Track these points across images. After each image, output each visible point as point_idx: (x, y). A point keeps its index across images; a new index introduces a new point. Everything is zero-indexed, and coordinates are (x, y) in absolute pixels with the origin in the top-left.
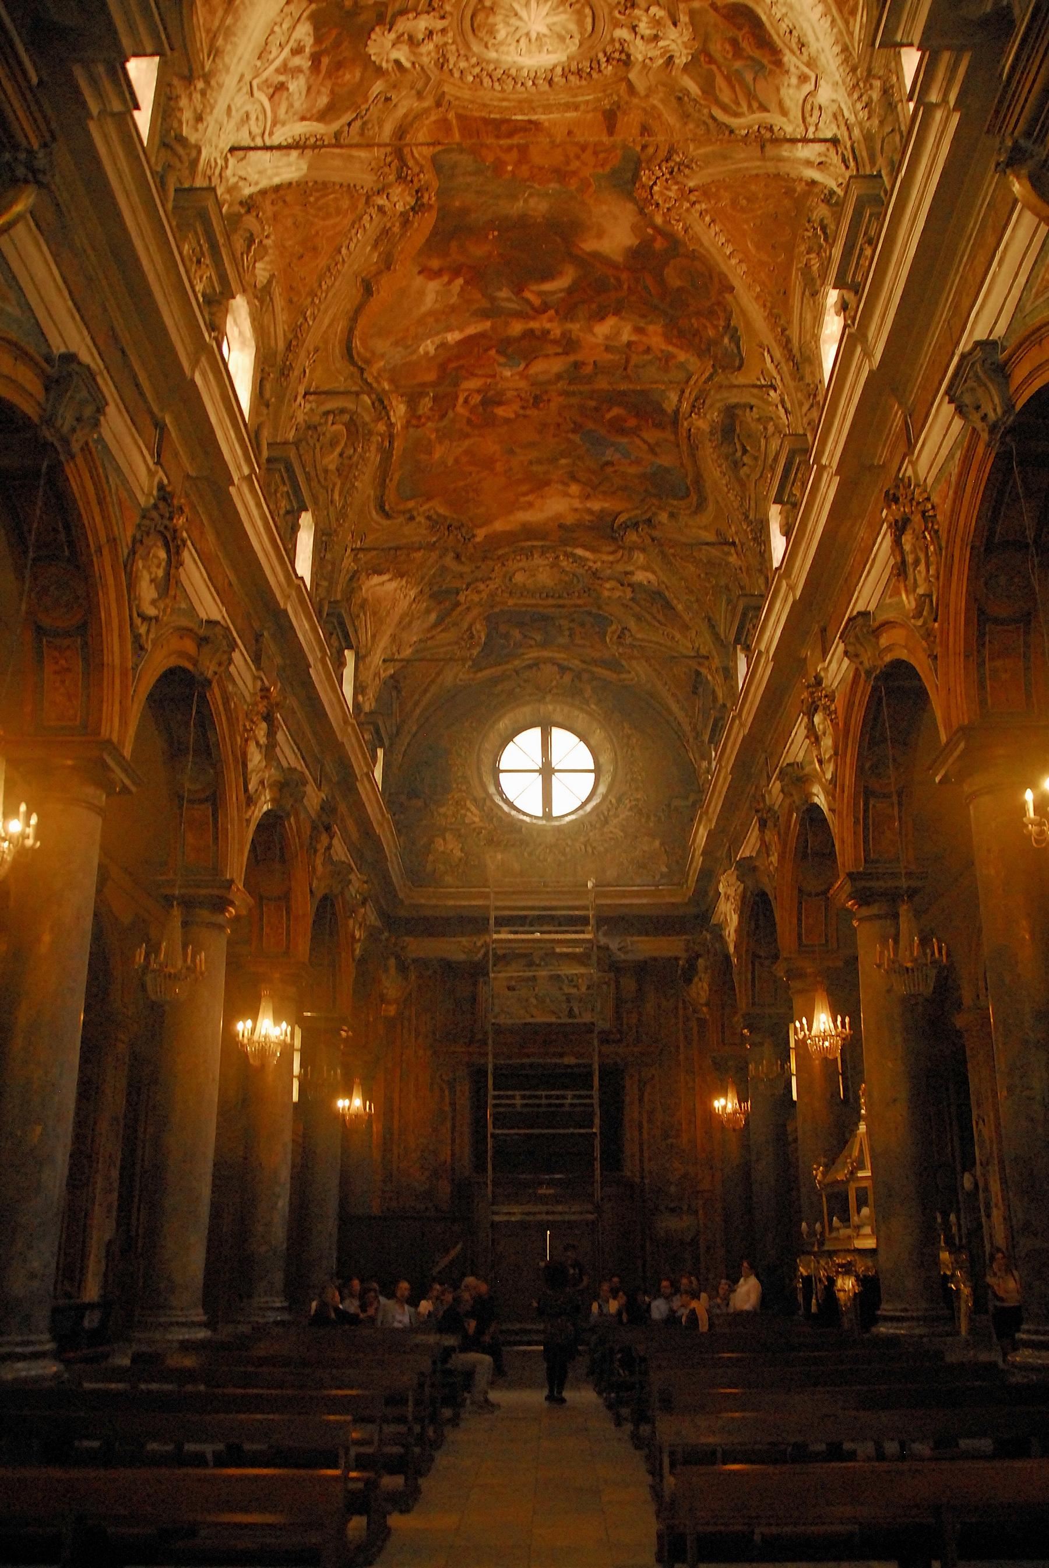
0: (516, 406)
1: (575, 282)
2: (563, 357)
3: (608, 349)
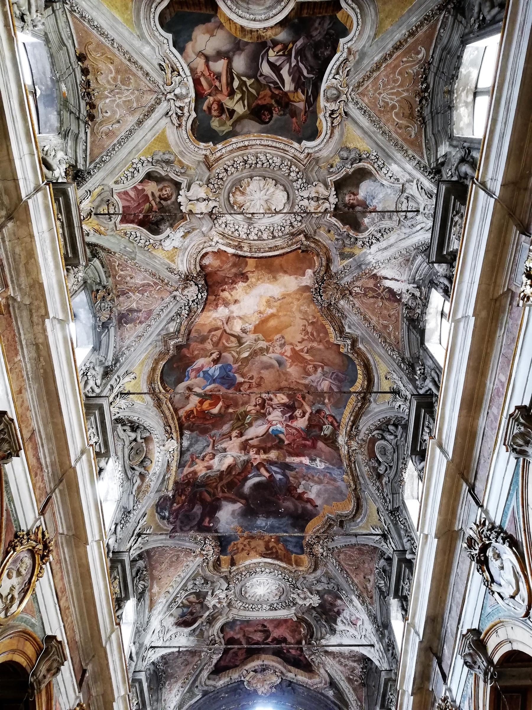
0: (275, 401)
1: (243, 485)
2: (249, 437)
3: (225, 450)
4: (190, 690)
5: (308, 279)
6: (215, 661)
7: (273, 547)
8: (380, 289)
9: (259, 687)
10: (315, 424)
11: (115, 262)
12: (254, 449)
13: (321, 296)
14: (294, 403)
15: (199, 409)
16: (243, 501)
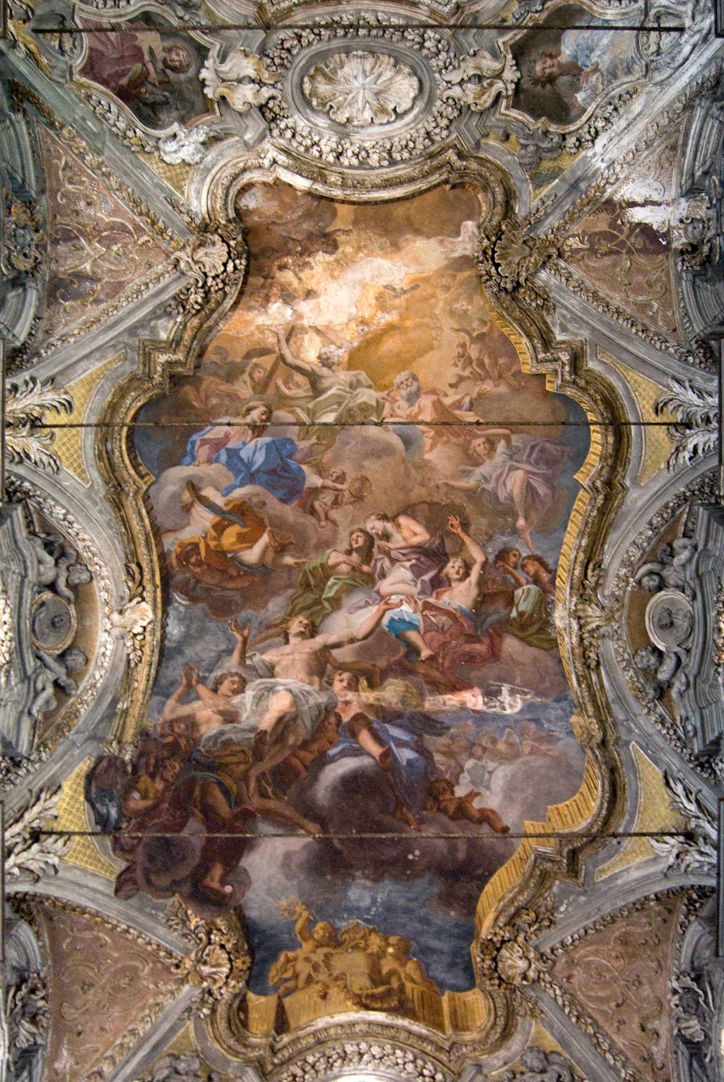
0: (398, 541)
1: (315, 778)
2: (333, 639)
3: (270, 670)
5: (467, 239)
7: (392, 973)
8: (621, 232)
10: (494, 593)
11: (59, 159)
12: (346, 676)
13: (497, 266)
14: (442, 543)
15: (212, 544)
16: (313, 827)
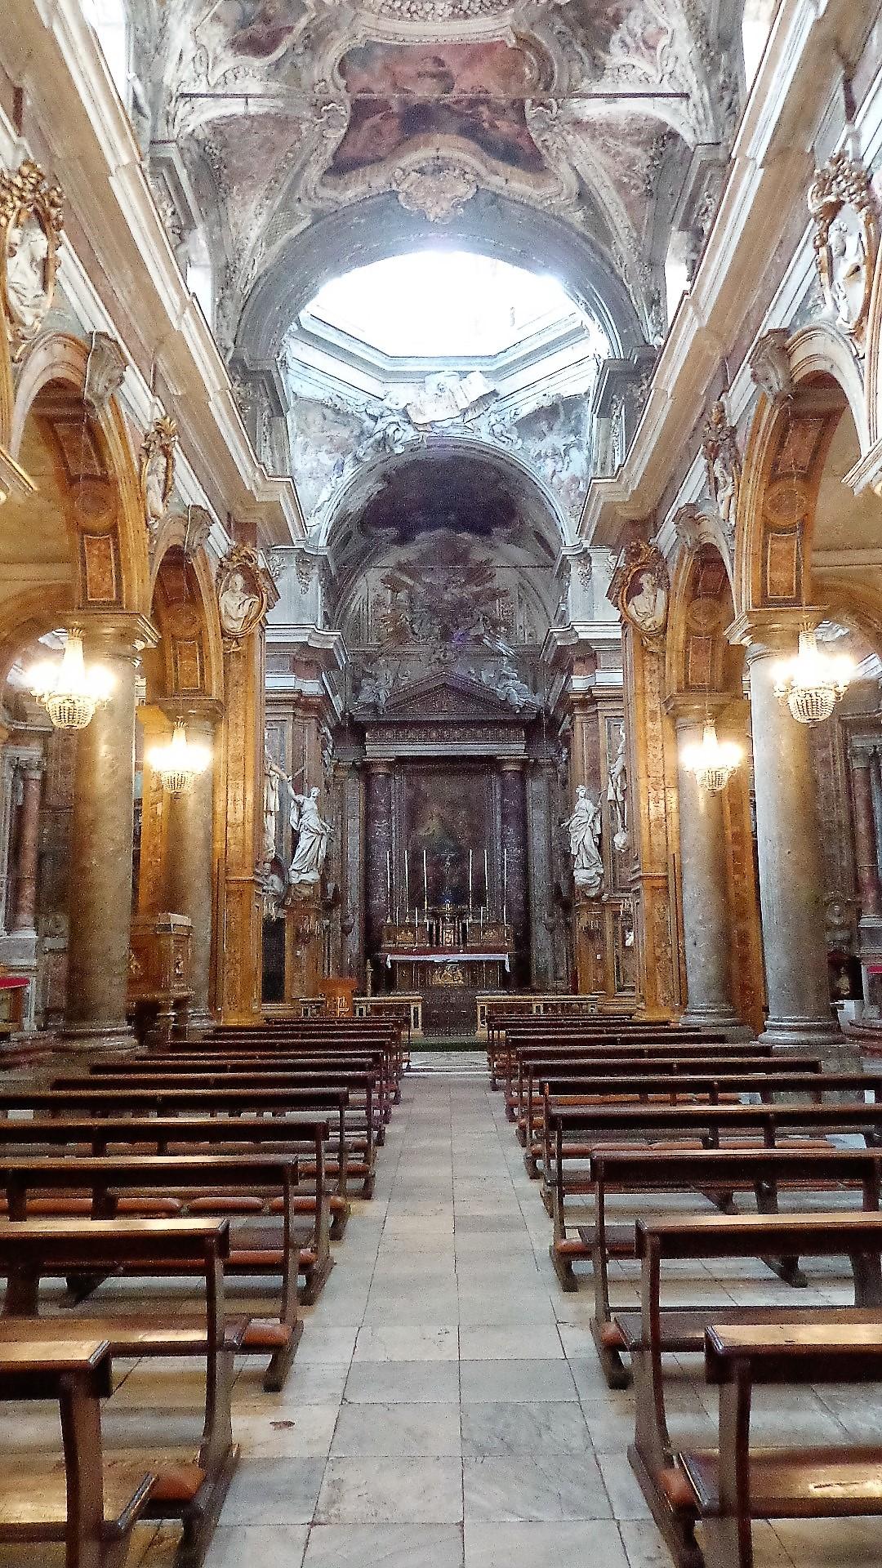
4: (285, 206)
6: (332, 146)
9: (429, 204)
